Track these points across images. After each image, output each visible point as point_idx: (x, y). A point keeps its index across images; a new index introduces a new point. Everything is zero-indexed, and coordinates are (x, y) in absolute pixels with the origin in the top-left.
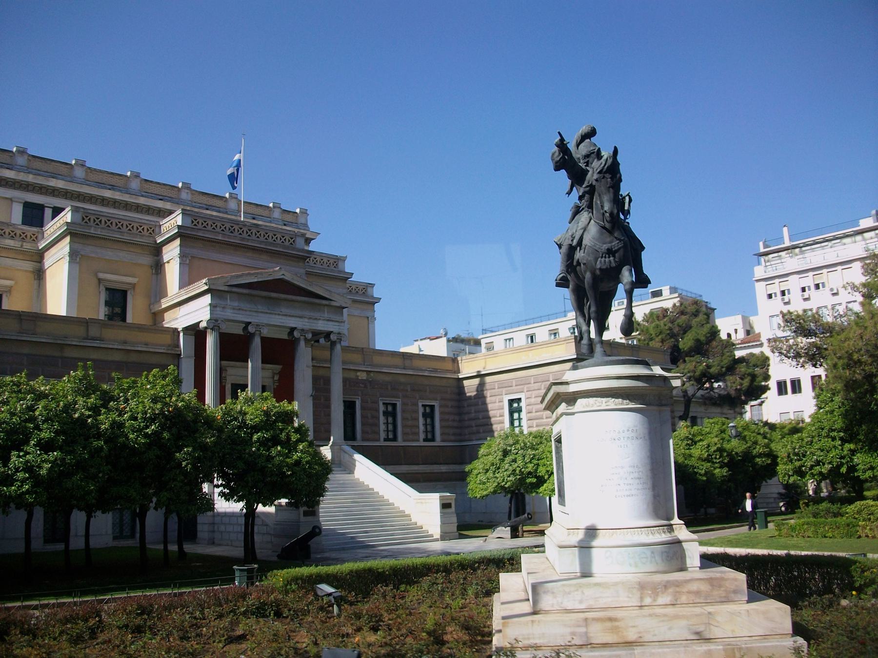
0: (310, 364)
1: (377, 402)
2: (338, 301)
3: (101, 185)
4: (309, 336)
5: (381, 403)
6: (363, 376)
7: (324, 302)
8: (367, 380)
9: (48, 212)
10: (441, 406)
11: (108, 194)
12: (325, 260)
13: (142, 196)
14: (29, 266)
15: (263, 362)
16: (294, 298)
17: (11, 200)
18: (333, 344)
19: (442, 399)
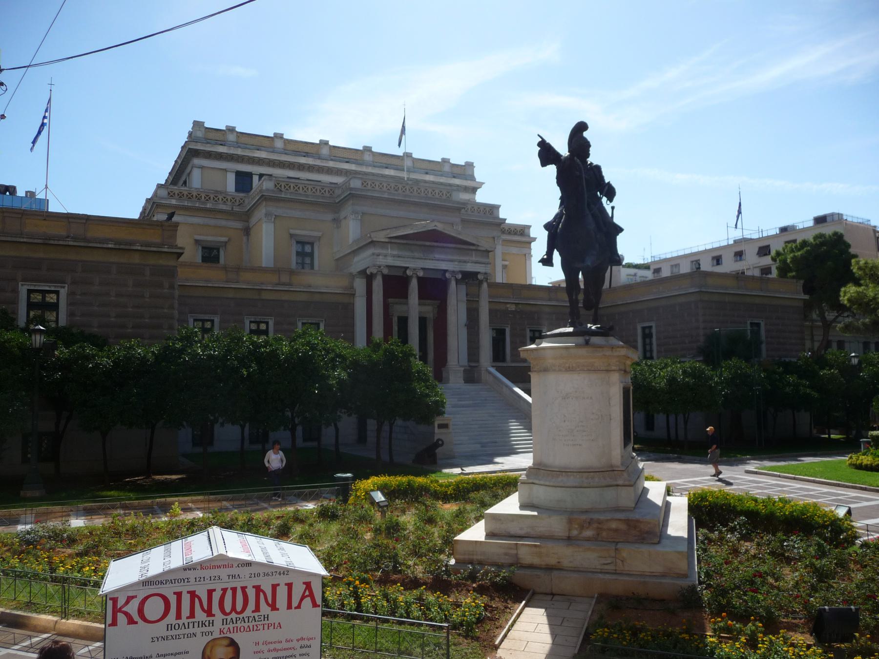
0: (465, 299)
2: (484, 245)
3: (297, 153)
4: (460, 276)
6: (512, 308)
7: (472, 247)
9: (255, 179)
11: (303, 160)
12: (482, 209)
13: (332, 160)
14: (239, 225)
15: (419, 298)
16: (445, 245)
17: (225, 170)
18: (481, 282)
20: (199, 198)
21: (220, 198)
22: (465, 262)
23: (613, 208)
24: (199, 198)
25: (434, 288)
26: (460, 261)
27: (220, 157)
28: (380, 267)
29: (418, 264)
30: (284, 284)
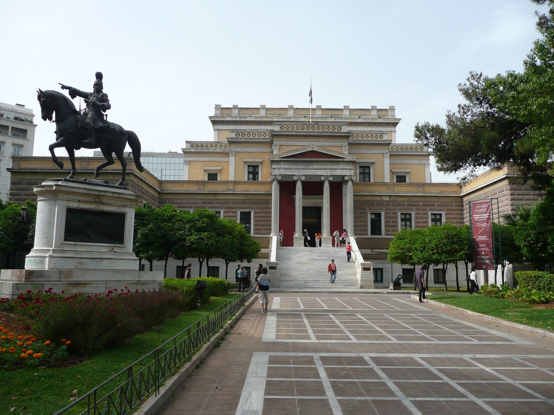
1: (396, 213)
8: (389, 201)
10: (446, 214)
15: (303, 194)
18: (347, 181)
19: (447, 210)
21: (219, 145)
22: (335, 169)
23: (106, 115)
25: (313, 188)
28: (276, 176)
29: (300, 172)
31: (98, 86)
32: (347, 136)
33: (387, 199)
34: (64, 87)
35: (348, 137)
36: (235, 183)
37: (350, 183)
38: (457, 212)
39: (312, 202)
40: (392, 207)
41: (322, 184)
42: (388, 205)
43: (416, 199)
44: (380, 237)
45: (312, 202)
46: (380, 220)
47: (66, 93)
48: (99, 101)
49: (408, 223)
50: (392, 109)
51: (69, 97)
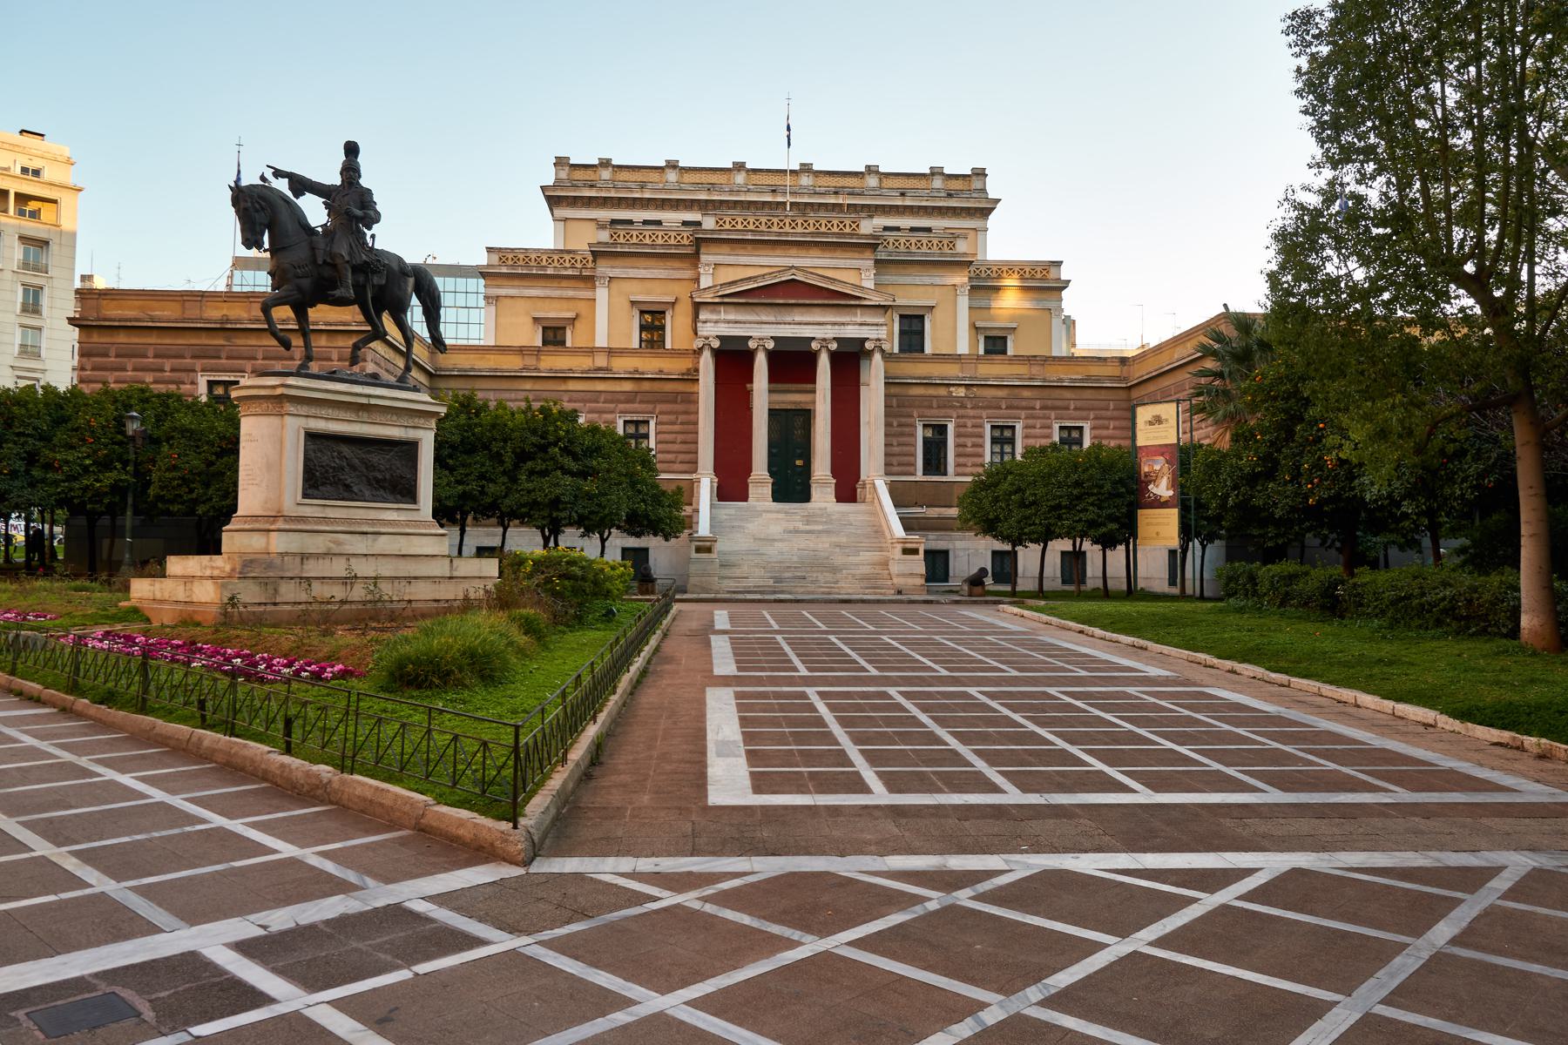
1: (981, 426)
5: (988, 427)
18: (869, 354)
20: (538, 260)
23: (373, 236)
24: (538, 260)
25: (792, 363)
26: (834, 324)
27: (589, 202)
29: (763, 330)
30: (600, 369)
31: (351, 170)
32: (870, 245)
33: (961, 392)
34: (278, 174)
35: (874, 247)
36: (611, 352)
37: (877, 357)
38: (1117, 423)
39: (792, 399)
40: (971, 413)
41: (812, 358)
42: (963, 407)
43: (1026, 393)
44: (944, 479)
45: (792, 399)
46: (945, 442)
47: (282, 185)
48: (353, 202)
49: (1007, 449)
50: (980, 173)
51: (290, 194)
